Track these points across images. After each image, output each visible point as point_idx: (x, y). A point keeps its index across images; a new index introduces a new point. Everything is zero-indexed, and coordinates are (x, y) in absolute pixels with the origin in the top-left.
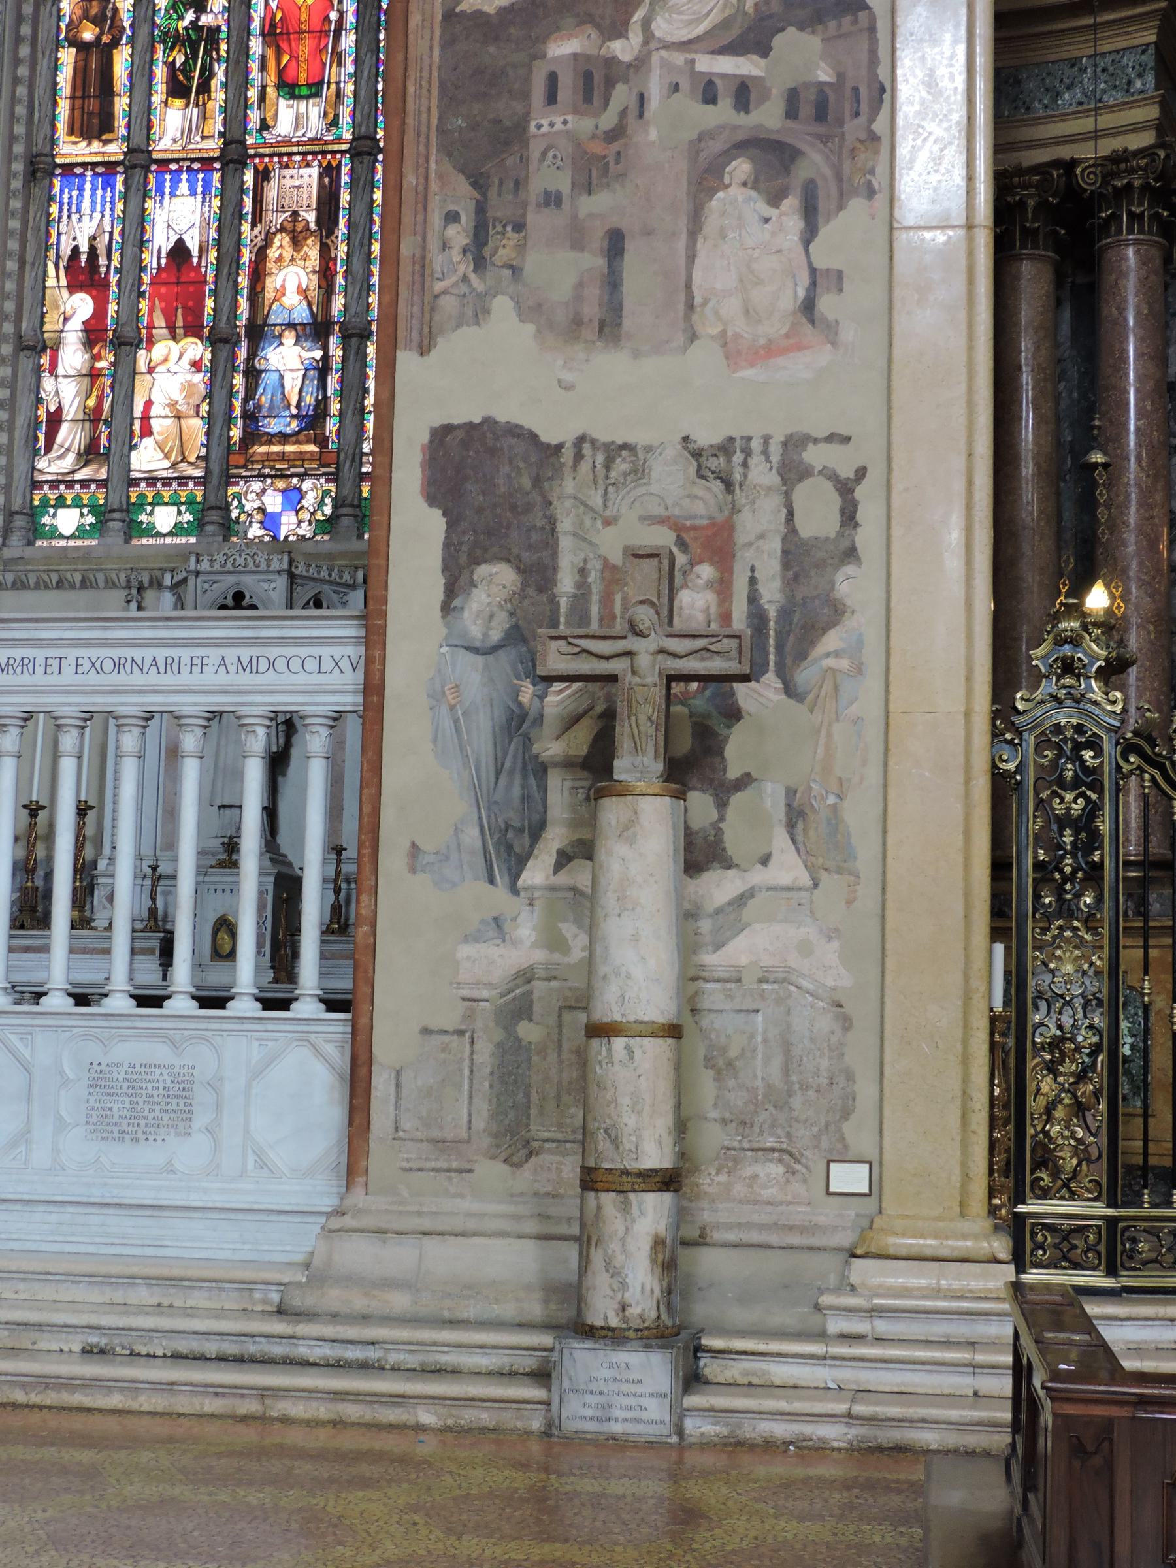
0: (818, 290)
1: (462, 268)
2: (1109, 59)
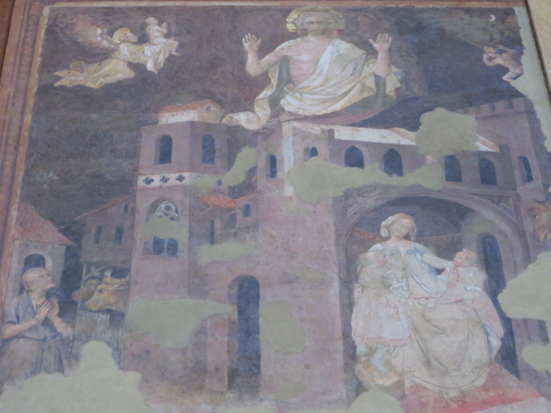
0: (518, 340)
1: (43, 312)
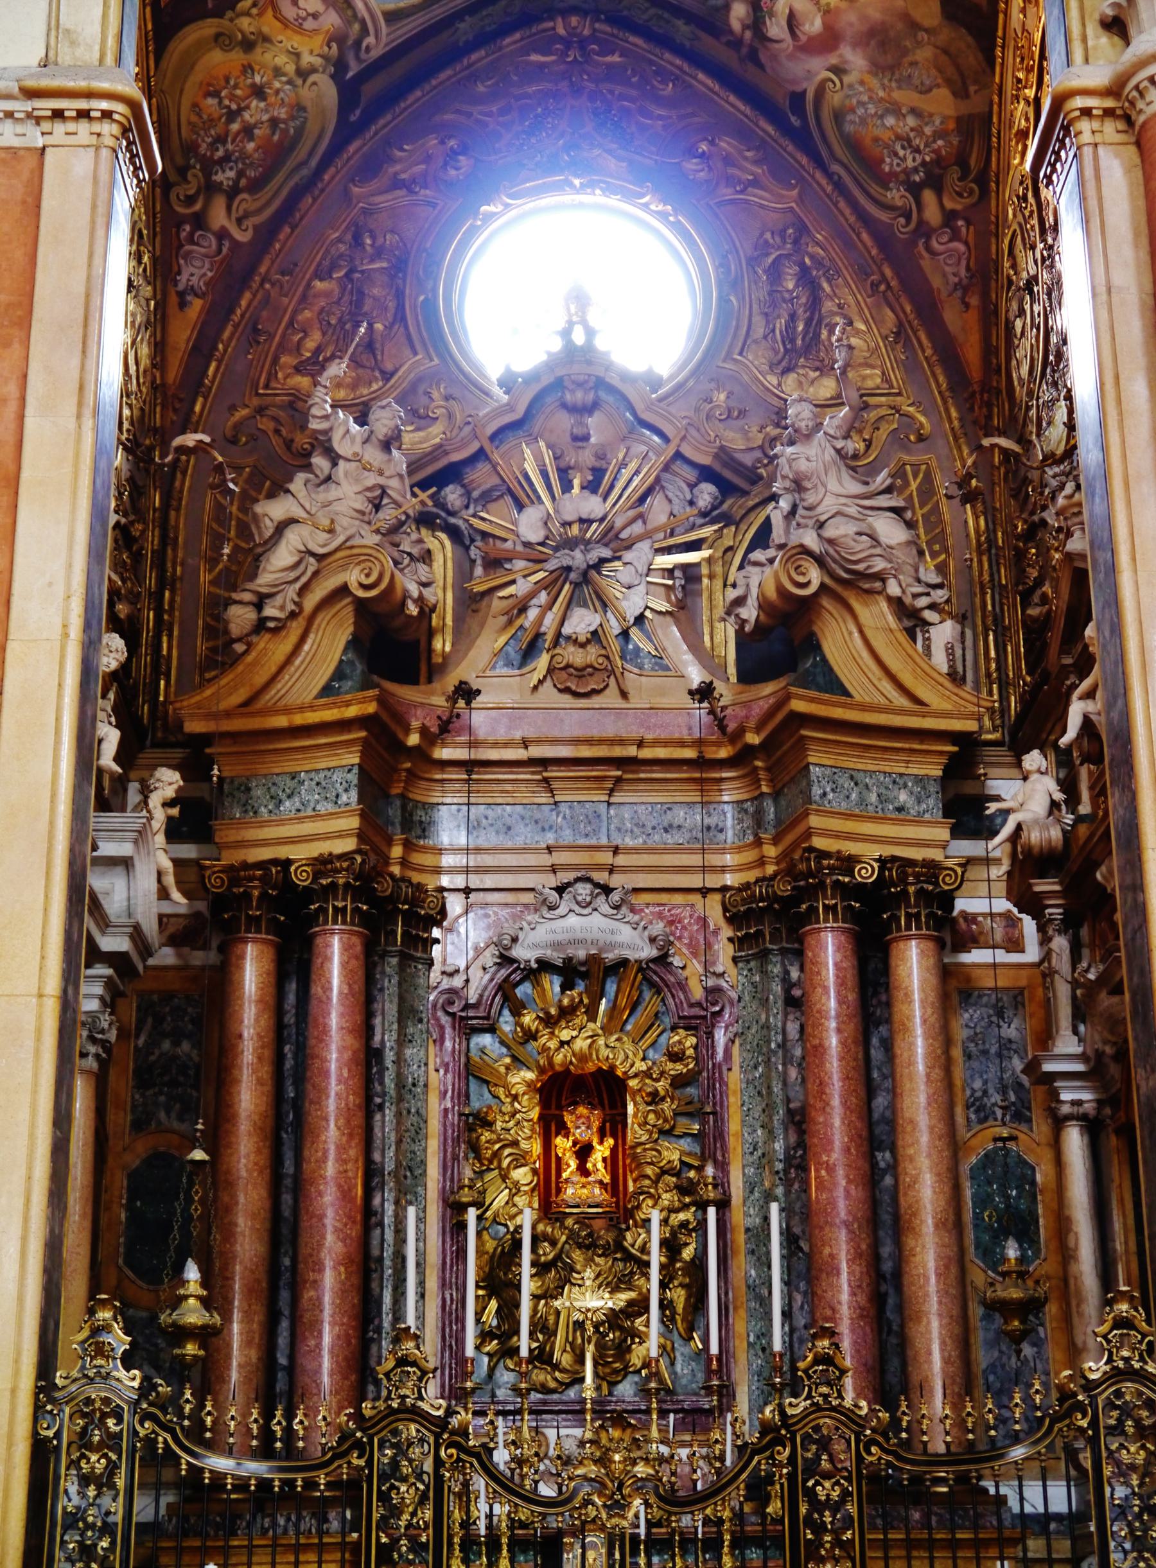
2: (322, 775)
